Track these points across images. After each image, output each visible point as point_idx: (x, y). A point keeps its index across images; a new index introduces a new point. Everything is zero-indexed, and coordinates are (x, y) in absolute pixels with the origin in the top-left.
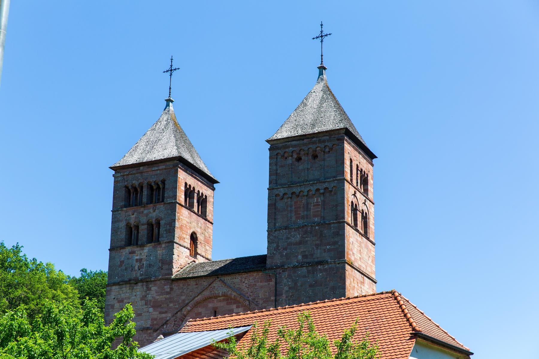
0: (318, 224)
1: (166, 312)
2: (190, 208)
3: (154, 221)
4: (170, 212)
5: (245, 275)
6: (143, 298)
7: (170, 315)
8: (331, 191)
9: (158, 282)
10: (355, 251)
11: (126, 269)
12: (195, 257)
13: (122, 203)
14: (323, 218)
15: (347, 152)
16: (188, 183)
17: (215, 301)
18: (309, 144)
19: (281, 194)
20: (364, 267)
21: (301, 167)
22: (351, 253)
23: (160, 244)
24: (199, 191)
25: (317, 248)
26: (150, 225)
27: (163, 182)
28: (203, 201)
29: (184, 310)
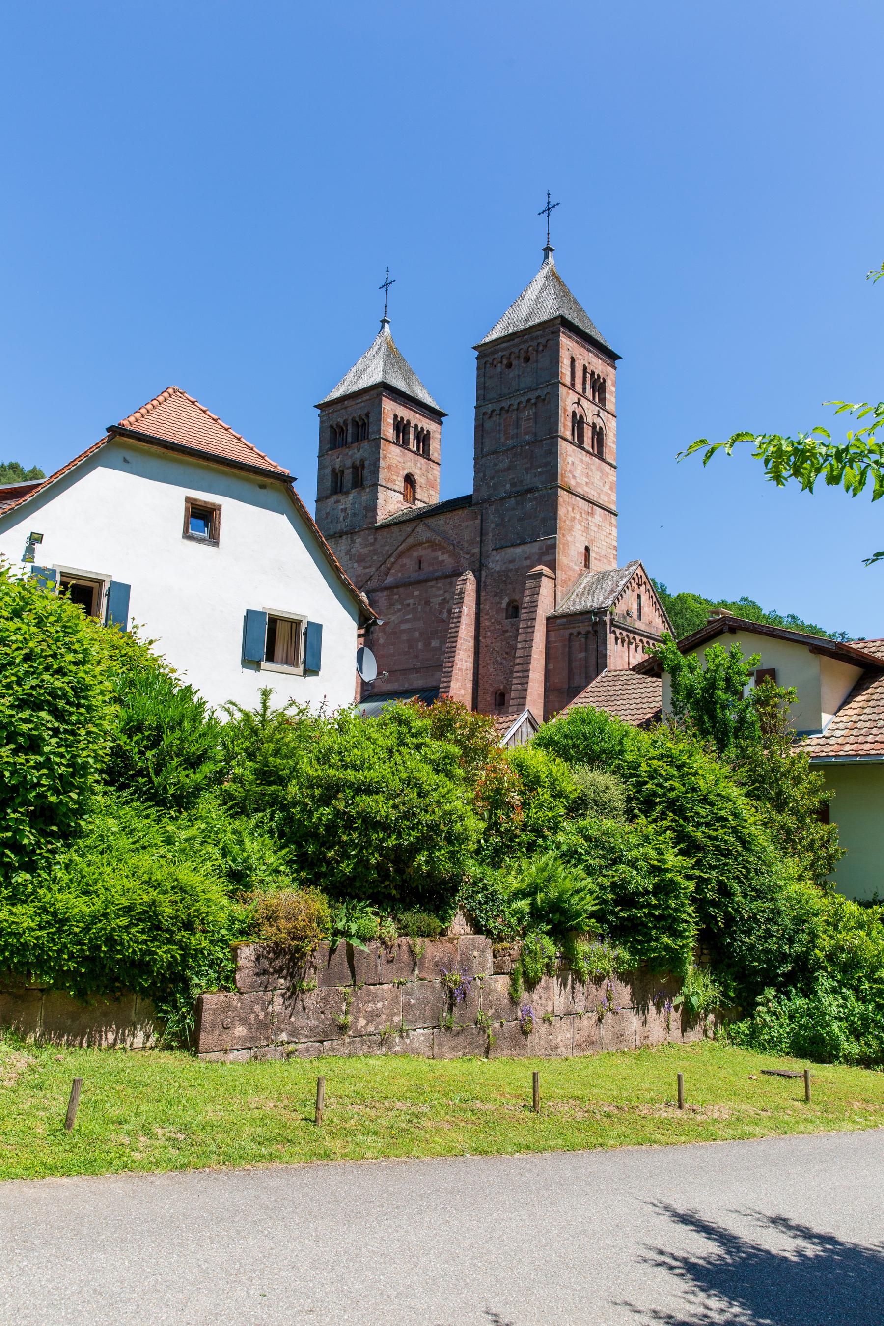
0: (529, 444)
1: (370, 567)
2: (405, 445)
3: (358, 463)
4: (374, 449)
5: (449, 515)
7: (374, 569)
8: (544, 400)
10: (577, 473)
11: (331, 522)
12: (414, 503)
13: (328, 446)
14: (535, 434)
15: (565, 348)
16: (400, 415)
17: (420, 548)
18: (520, 344)
19: (489, 412)
20: (595, 494)
21: (511, 375)
22: (570, 476)
23: (364, 488)
24: (416, 426)
26: (354, 467)
27: (367, 415)
28: (423, 438)
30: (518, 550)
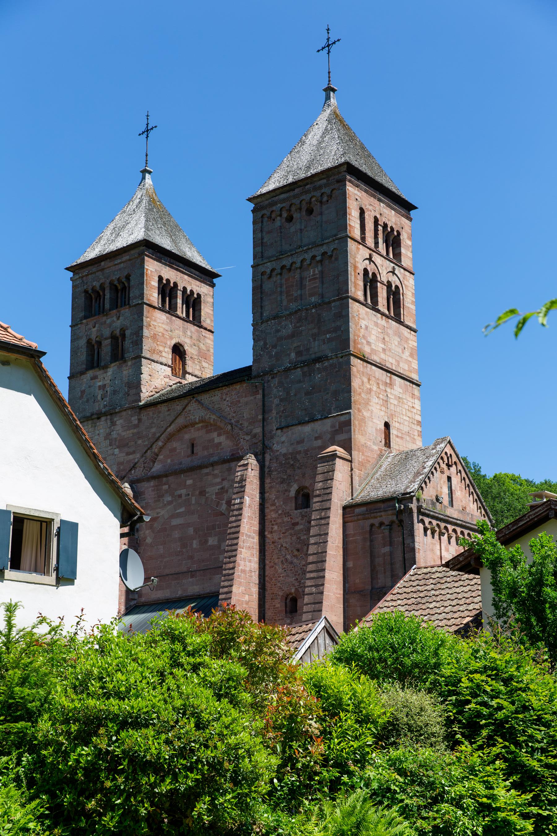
0: (315, 306)
1: (134, 452)
2: (172, 311)
3: (118, 332)
4: (136, 316)
5: (225, 390)
6: (108, 436)
7: (138, 455)
8: (331, 256)
9: (124, 413)
10: (372, 339)
11: (88, 401)
12: (184, 377)
13: (82, 314)
14: (322, 296)
15: (353, 198)
16: (165, 276)
17: (192, 430)
18: (302, 194)
19: (268, 271)
20: (394, 362)
21: (292, 230)
22: (365, 342)
23: (125, 361)
24: (185, 288)
25: (314, 340)
26: (113, 337)
27: (128, 278)
28: (193, 303)
29: (154, 447)
30: (307, 429)
